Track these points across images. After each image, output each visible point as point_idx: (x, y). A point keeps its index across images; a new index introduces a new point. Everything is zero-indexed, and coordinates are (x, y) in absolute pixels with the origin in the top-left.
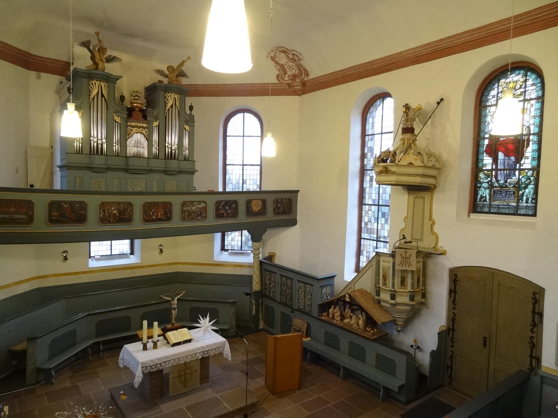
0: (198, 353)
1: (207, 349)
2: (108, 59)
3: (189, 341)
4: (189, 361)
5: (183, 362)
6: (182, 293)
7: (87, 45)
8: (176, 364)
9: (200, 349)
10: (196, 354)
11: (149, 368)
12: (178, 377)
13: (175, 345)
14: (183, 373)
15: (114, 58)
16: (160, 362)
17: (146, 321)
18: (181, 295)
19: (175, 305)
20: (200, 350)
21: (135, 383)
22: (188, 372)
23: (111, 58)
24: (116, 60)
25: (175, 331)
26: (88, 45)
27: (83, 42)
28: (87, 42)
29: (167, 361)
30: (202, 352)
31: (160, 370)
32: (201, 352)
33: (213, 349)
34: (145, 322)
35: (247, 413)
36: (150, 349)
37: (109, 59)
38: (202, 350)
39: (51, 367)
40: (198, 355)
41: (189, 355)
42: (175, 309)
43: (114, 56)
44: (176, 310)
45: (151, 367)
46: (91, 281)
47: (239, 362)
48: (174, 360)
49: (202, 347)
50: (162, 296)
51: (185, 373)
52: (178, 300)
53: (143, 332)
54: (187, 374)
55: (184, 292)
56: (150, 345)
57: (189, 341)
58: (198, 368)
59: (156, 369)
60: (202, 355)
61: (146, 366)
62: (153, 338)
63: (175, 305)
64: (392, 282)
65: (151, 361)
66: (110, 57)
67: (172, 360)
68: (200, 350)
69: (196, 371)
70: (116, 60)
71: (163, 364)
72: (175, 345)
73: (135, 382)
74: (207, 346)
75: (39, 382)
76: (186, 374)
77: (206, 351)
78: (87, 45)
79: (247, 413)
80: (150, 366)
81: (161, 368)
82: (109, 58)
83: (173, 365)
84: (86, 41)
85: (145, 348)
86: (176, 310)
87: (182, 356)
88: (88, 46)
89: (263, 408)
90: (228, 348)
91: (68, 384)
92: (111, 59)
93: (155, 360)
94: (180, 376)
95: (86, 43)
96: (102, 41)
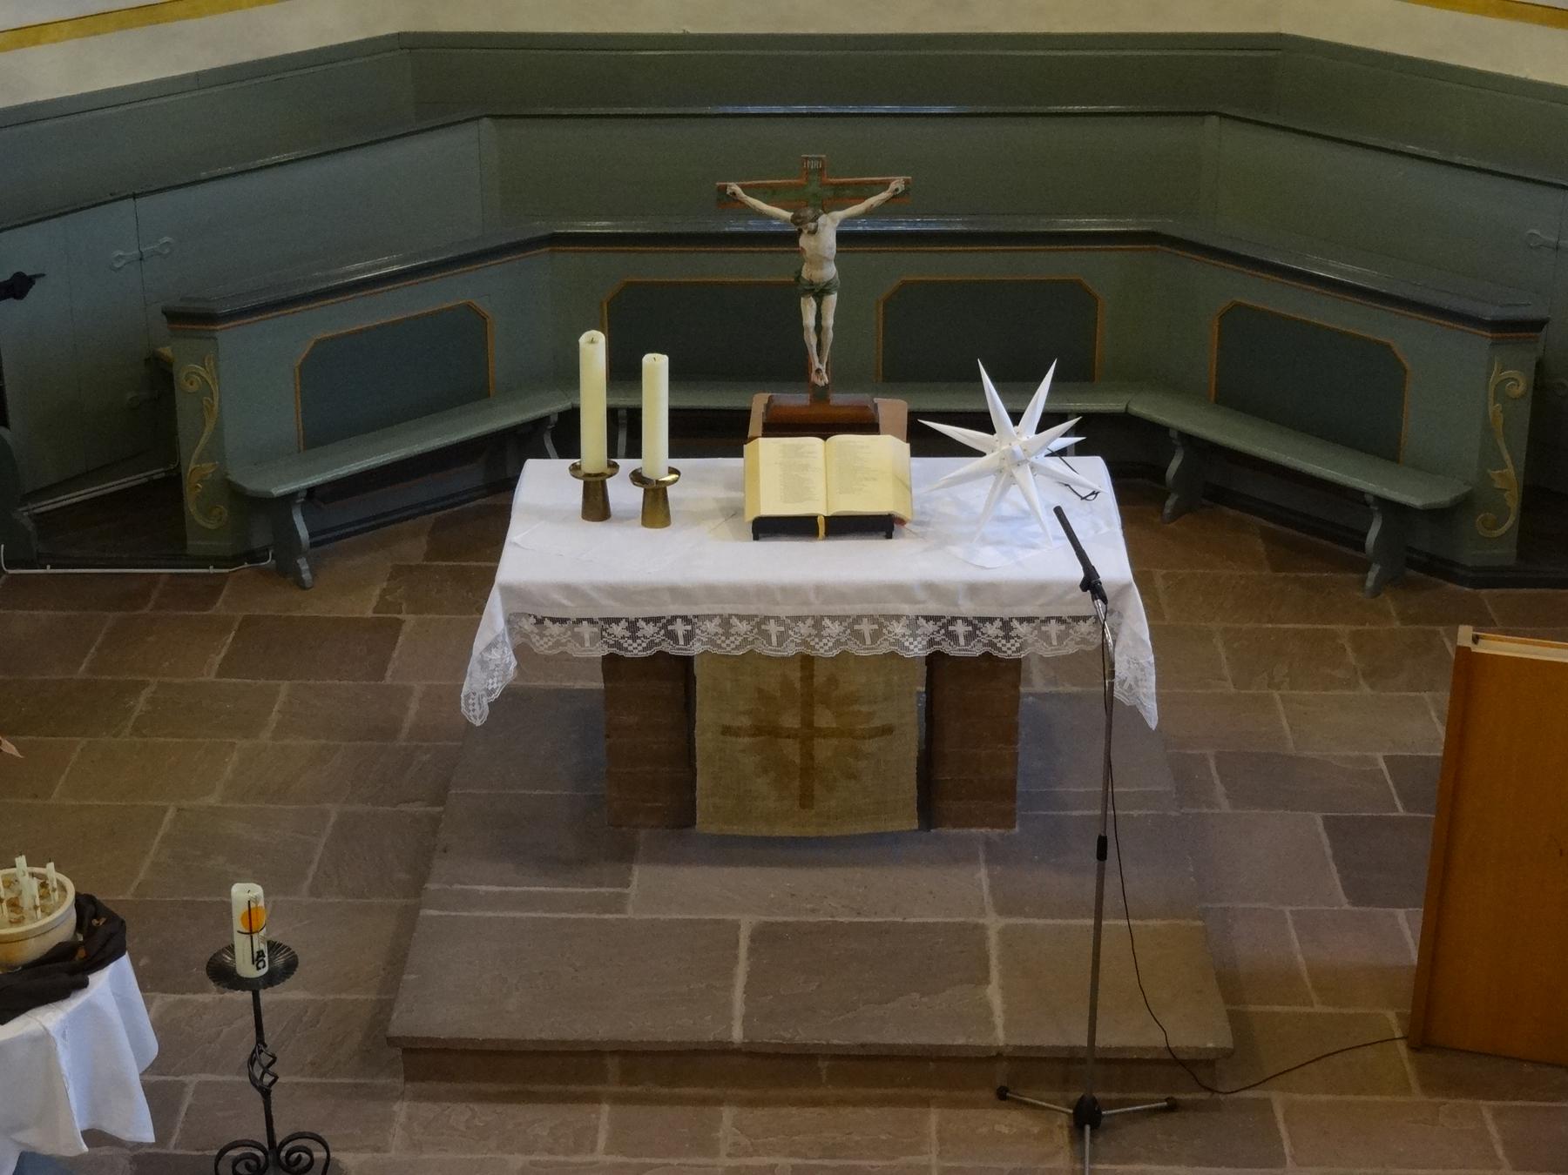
0: (898, 618)
1: (968, 608)
3: (881, 526)
4: (835, 652)
5: (791, 650)
6: (885, 186)
8: (644, 654)
9: (812, 597)
10: (882, 621)
11: (649, 629)
12: (757, 731)
13: (767, 528)
14: (791, 721)
16: (632, 612)
17: (601, 338)
18: (873, 201)
19: (820, 261)
20: (913, 601)
21: (468, 697)
22: (824, 719)
25: (814, 443)
29: (1048, 619)
30: (936, 619)
31: (1002, 660)
32: (928, 618)
33: (554, 620)
34: (592, 342)
35: (1099, 1095)
36: (625, 518)
38: (933, 608)
39: (279, 490)
40: (899, 629)
41: (833, 618)
42: (820, 292)
44: (832, 300)
45: (944, 626)
46: (691, 30)
47: (1379, 756)
48: (726, 622)
49: (932, 589)
50: (735, 187)
51: (808, 723)
52: (842, 238)
53: (1045, 406)
54: (819, 730)
55: (897, 184)
56: (624, 494)
57: (881, 526)
58: (907, 714)
59: (977, 650)
60: (931, 642)
61: (632, 617)
62: (639, 456)
63: (820, 261)
64: (612, 413)
65: (571, 590)
67: (710, 617)
68: (913, 601)
69: (887, 730)
71: (1021, 629)
72: (767, 528)
73: (465, 689)
74: (974, 590)
75: (253, 556)
76: (809, 734)
77: (966, 620)
79: (1095, 1101)
80: (656, 620)
81: (1008, 650)
83: (716, 651)
85: (596, 506)
86: (832, 300)
87: (785, 611)
89: (1265, 1106)
90: (1138, 640)
91: (365, 606)
93: (594, 595)
94: (767, 731)
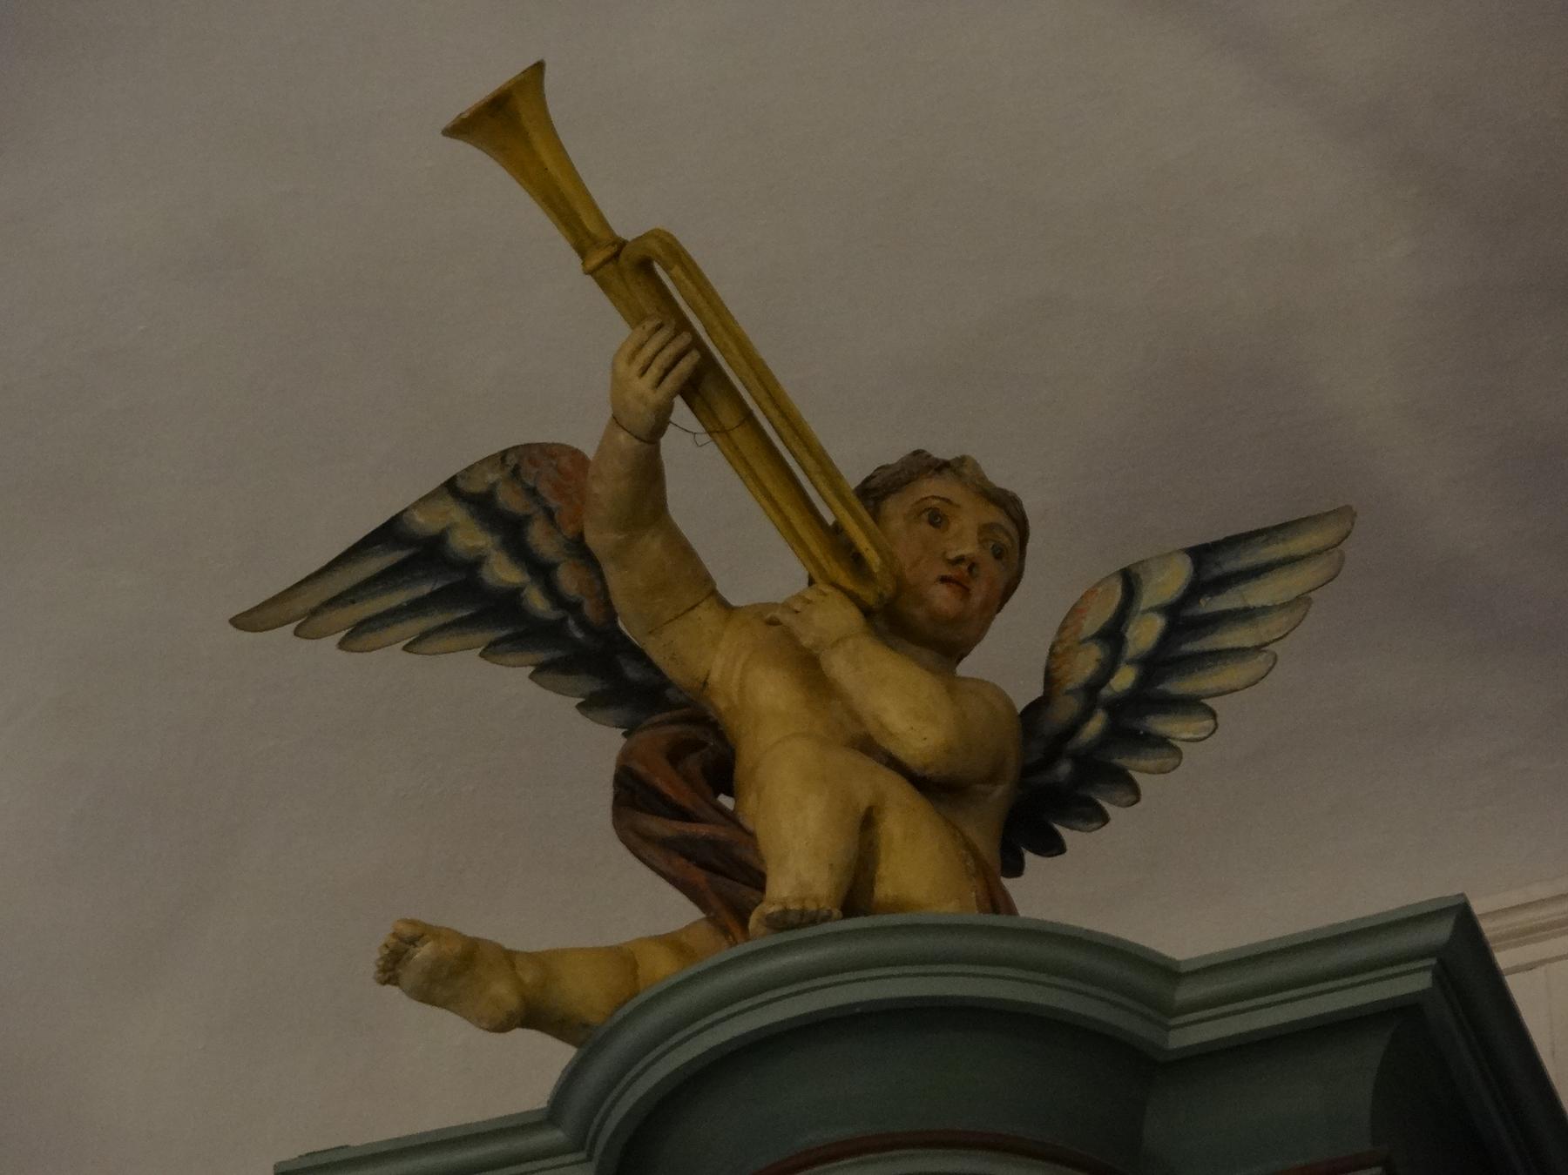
2: (1092, 689)
7: (503, 572)
15: (1210, 605)
23: (1144, 633)
24: (1247, 615)
26: (542, 571)
27: (389, 533)
28: (483, 506)
37: (1124, 679)
43: (1200, 555)
66: (1113, 635)
70: (1247, 615)
78: (503, 572)
82: (1108, 669)
84: (451, 487)
88: (537, 602)
92: (1156, 664)
95: (469, 537)
96: (676, 254)
